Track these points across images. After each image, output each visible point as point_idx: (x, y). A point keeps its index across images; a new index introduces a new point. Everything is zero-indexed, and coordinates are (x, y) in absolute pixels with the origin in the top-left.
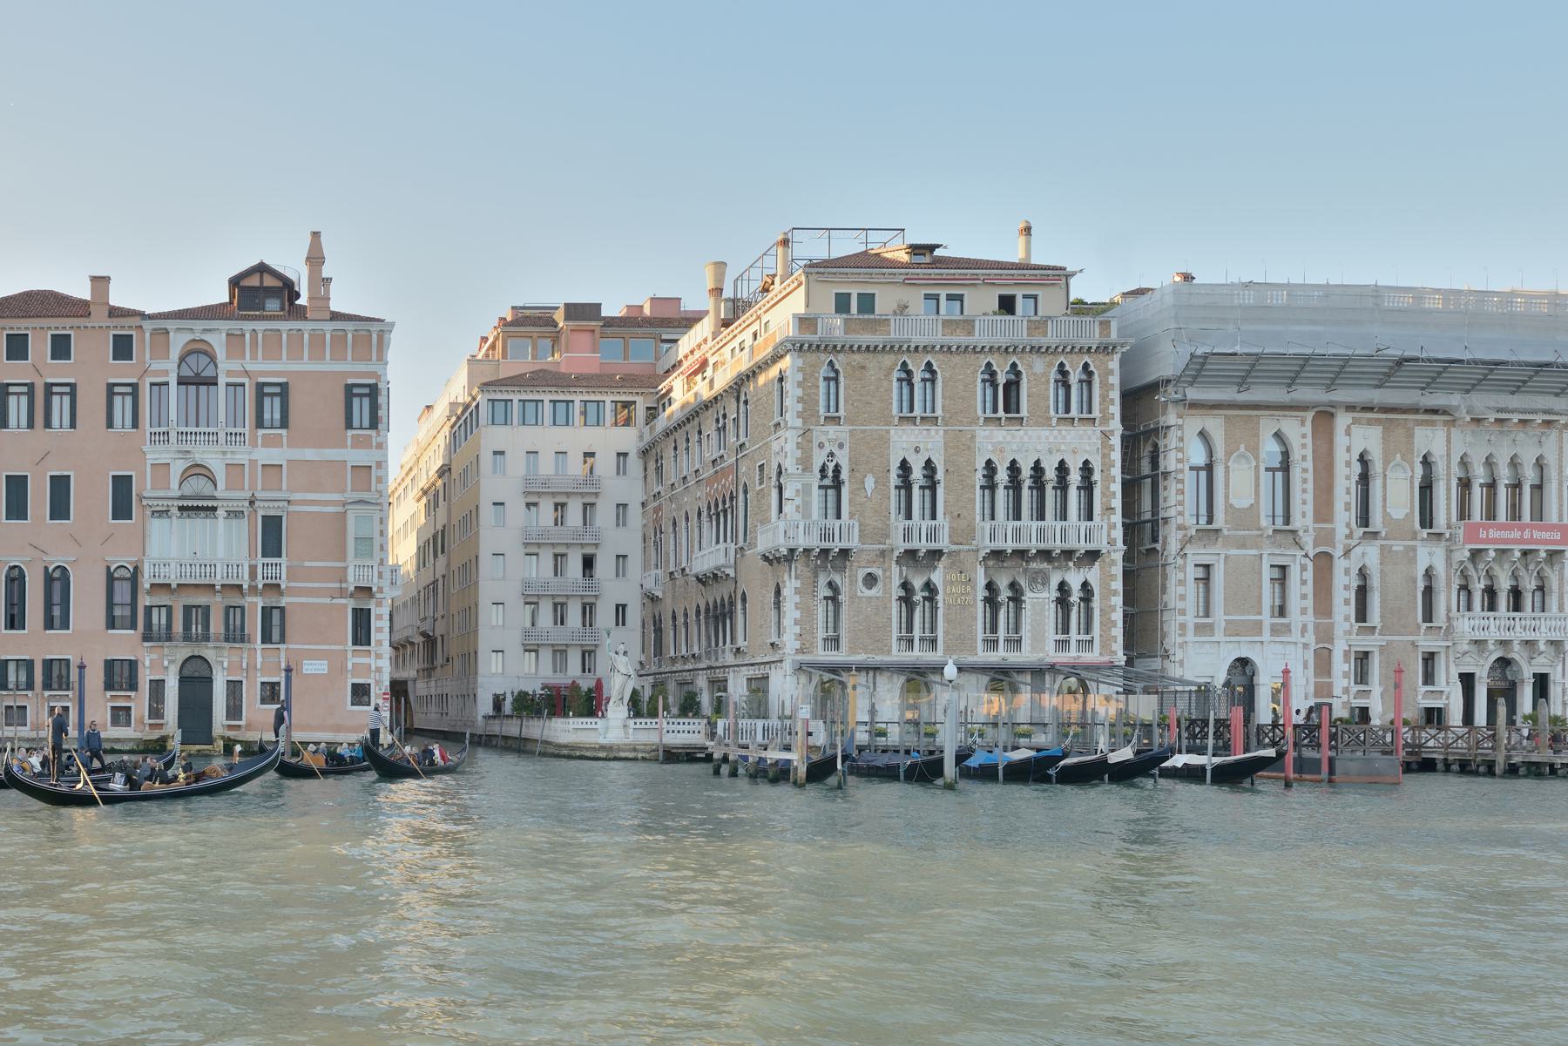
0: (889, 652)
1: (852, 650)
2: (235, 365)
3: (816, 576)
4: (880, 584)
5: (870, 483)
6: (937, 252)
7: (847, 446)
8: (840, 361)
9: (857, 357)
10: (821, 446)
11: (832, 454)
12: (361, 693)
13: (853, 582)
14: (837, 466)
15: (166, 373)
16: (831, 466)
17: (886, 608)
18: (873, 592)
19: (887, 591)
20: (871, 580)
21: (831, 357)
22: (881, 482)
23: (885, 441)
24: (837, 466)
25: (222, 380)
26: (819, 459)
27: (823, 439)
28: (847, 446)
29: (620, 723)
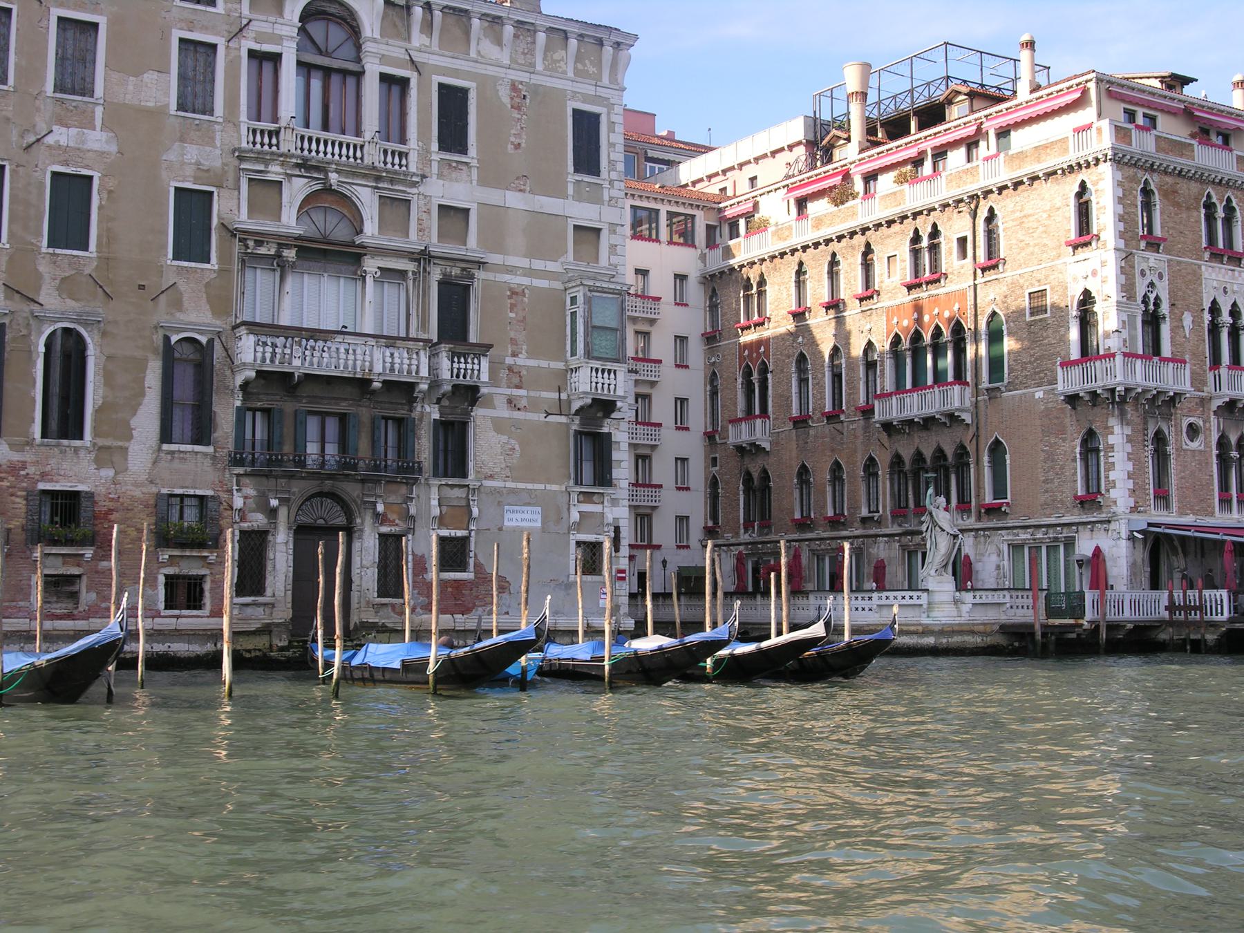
0: (1212, 514)
1: (1181, 513)
2: (396, 50)
3: (1146, 423)
4: (1201, 437)
5: (1187, 320)
6: (1188, 90)
7: (1166, 278)
8: (1154, 181)
9: (1169, 180)
10: (1143, 273)
11: (1152, 285)
12: (591, 558)
13: (1178, 433)
14: (1157, 298)
15: (279, 39)
16: (1152, 297)
17: (1208, 464)
18: (1195, 445)
19: (1208, 445)
20: (1193, 431)
21: (1147, 176)
22: (1197, 321)
23: (1197, 277)
24: (1157, 298)
25: (373, 69)
26: (1141, 289)
27: (1144, 266)
28: (1166, 278)
29: (947, 597)
